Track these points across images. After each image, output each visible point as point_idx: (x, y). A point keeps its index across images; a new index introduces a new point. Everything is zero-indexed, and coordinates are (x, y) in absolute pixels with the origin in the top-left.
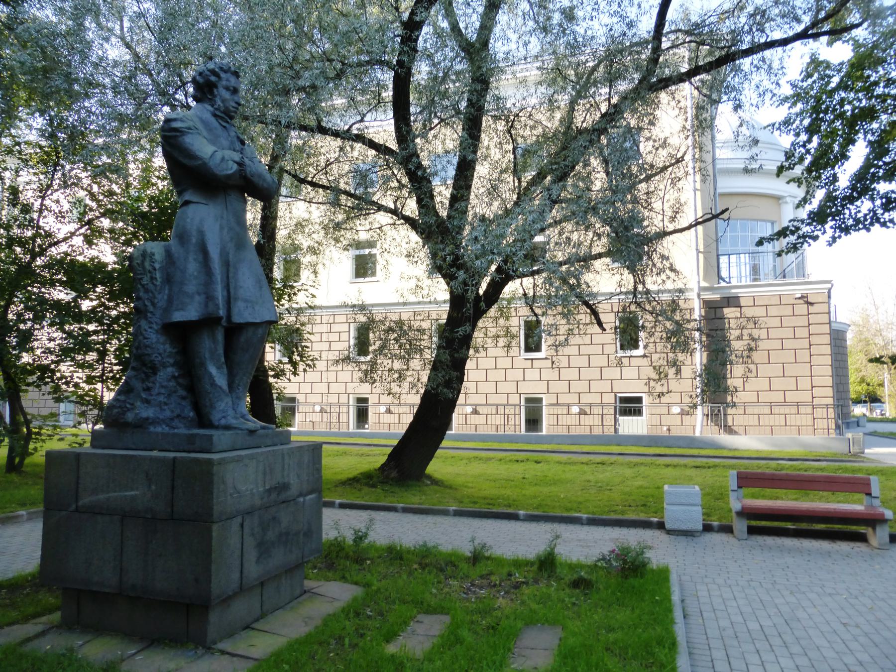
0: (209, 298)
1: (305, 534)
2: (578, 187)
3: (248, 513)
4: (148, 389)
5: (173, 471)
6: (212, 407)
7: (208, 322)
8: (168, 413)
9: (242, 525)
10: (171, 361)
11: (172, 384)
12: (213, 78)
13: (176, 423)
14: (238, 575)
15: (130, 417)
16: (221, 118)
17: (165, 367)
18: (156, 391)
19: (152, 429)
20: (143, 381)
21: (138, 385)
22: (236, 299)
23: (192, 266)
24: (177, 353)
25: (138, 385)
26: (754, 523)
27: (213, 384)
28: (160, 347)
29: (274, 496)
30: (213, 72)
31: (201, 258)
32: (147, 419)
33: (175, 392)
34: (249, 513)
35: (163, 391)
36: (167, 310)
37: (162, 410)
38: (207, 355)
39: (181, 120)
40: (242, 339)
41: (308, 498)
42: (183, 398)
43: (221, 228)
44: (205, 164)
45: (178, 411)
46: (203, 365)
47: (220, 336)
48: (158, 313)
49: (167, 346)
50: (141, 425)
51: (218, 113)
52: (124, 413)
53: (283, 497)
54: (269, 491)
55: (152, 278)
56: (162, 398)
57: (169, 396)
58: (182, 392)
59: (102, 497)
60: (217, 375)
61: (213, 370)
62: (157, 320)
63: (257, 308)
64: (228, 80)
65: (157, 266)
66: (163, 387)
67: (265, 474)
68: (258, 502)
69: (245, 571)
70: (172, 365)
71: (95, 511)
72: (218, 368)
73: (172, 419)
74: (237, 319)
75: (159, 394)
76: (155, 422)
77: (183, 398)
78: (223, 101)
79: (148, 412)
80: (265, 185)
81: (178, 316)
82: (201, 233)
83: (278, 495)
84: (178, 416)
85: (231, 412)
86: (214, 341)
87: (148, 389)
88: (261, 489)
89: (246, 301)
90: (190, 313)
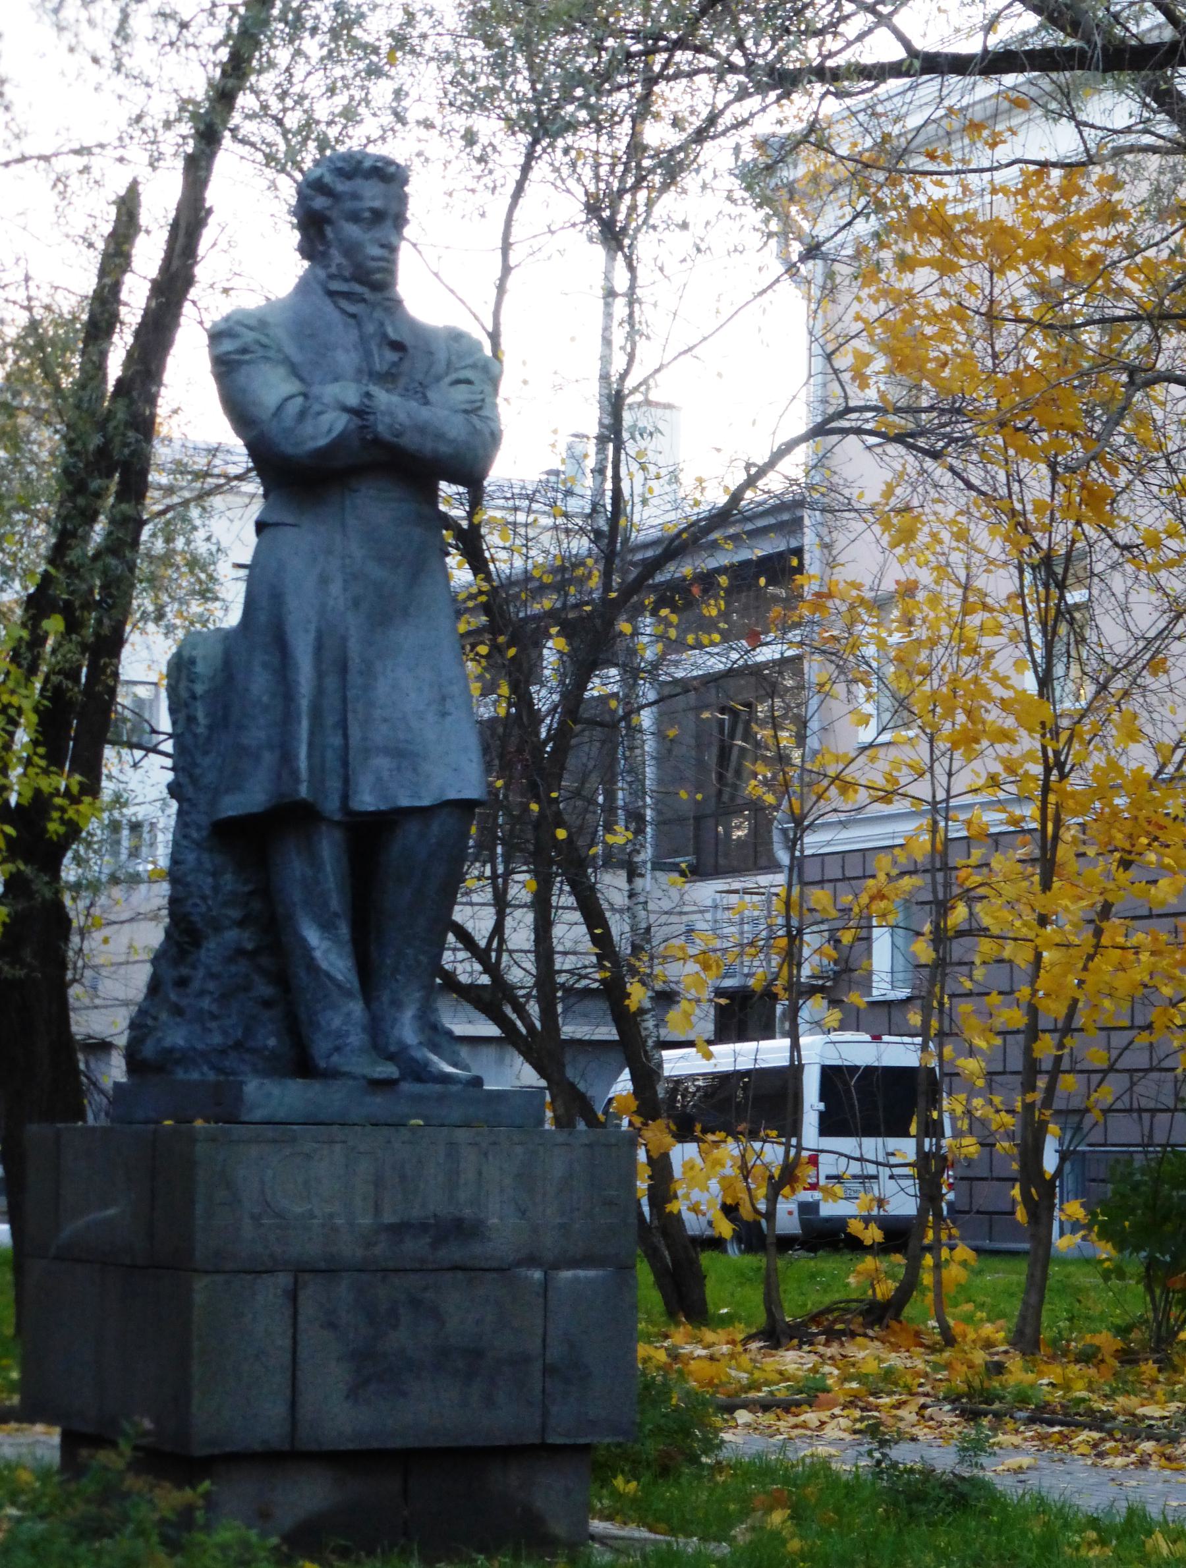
0: (287, 757)
1: (549, 1370)
8: (217, 1039)
9: (293, 1296)
10: (235, 914)
11: (242, 967)
16: (347, 295)
18: (196, 985)
19: (180, 1074)
23: (259, 683)
29: (416, 1247)
32: (171, 1050)
33: (247, 989)
34: (330, 1269)
35: (211, 986)
38: (297, 895)
41: (567, 1274)
42: (267, 1004)
47: (330, 848)
51: (335, 286)
53: (453, 1252)
54: (399, 1230)
56: (206, 1003)
58: (265, 989)
59: (80, 1223)
61: (313, 936)
64: (355, 196)
65: (199, 689)
66: (212, 976)
67: (378, 1182)
68: (350, 1249)
70: (241, 924)
73: (223, 1052)
74: (367, 800)
75: (202, 993)
77: (267, 1004)
80: (444, 449)
81: (233, 806)
83: (435, 1246)
84: (238, 1045)
86: (314, 861)
88: (366, 1221)
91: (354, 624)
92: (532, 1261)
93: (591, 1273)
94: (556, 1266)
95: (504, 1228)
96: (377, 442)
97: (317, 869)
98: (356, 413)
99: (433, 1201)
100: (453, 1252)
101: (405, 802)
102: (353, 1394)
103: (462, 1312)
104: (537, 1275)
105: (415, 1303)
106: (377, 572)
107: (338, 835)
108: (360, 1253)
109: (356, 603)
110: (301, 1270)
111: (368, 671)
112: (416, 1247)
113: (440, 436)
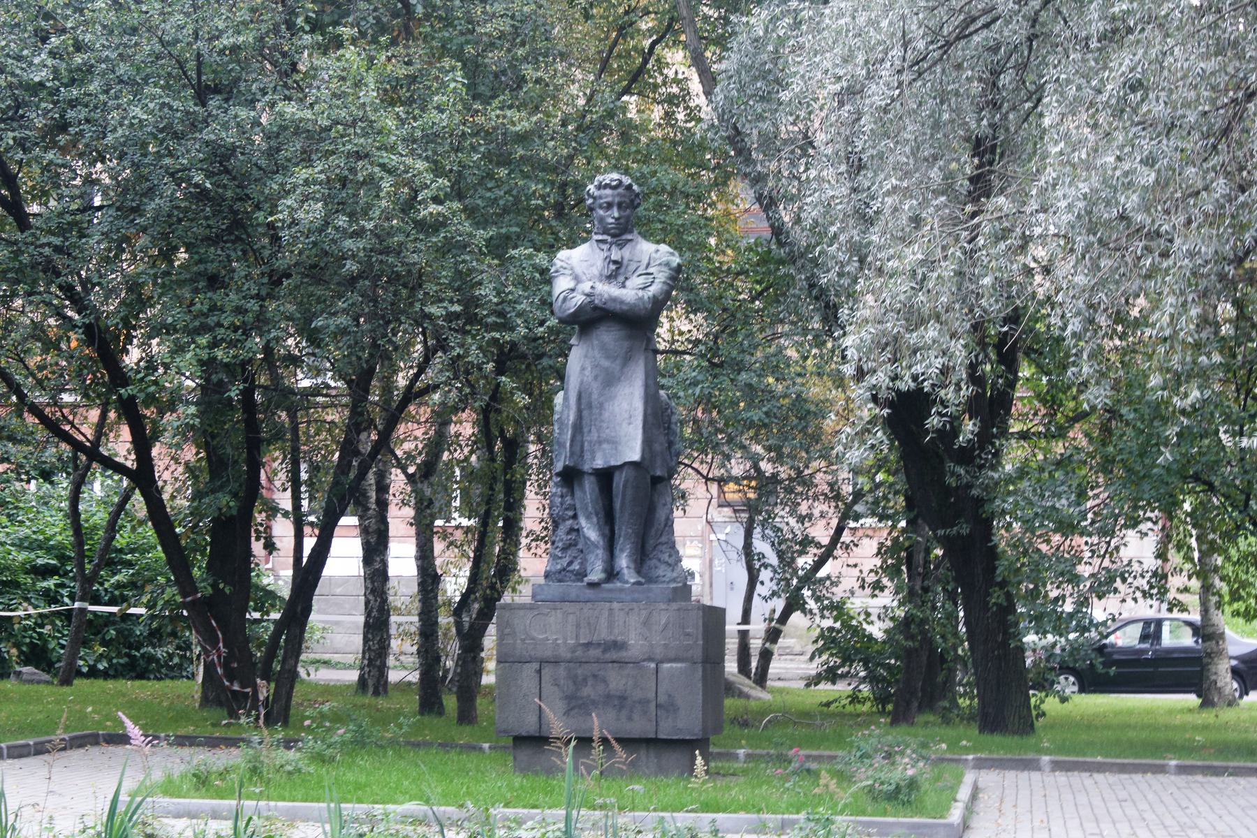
9: (539, 672)
17: (564, 520)
29: (594, 653)
53: (613, 655)
54: (588, 645)
67: (578, 626)
68: (564, 653)
72: (588, 518)
80: (625, 308)
83: (604, 652)
91: (595, 387)
92: (650, 659)
93: (679, 665)
94: (662, 662)
95: (636, 643)
96: (596, 308)
98: (588, 295)
99: (603, 634)
100: (613, 655)
101: (613, 463)
102: (567, 713)
103: (617, 681)
104: (653, 665)
105: (595, 676)
106: (606, 363)
107: (592, 478)
108: (569, 655)
109: (596, 378)
110: (543, 662)
111: (601, 406)
112: (594, 653)
113: (622, 302)
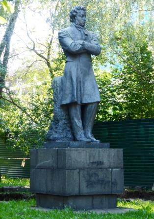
0: (73, 95)
1: (112, 183)
2: (32, 89)
3: (82, 169)
4: (56, 128)
5: (57, 153)
6: (77, 134)
7: (73, 104)
8: (62, 136)
9: (79, 172)
10: (64, 118)
11: (65, 125)
12: (74, 14)
13: (65, 139)
14: (78, 189)
15: (51, 137)
16: (78, 27)
17: (62, 120)
18: (58, 128)
19: (57, 141)
20: (55, 125)
21: (54, 127)
22: (84, 95)
23: (68, 85)
24: (66, 115)
25: (54, 127)
26: (125, 148)
27: (76, 125)
28: (61, 113)
29: (95, 166)
30: (74, 11)
31: (70, 81)
32: (55, 138)
33: (65, 129)
34: (83, 169)
35: (61, 128)
36: (61, 100)
37: (60, 135)
38: (74, 115)
39: (63, 33)
40: (88, 109)
41: (114, 169)
42: (69, 131)
43: (77, 69)
44: (69, 48)
45: (65, 135)
46: (73, 119)
47: (78, 108)
48: (59, 101)
49: (63, 113)
50: (55, 139)
51: (77, 26)
52: (50, 136)
54: (93, 163)
55: (57, 90)
56: (60, 131)
57: (63, 130)
58: (69, 129)
59: (42, 163)
60: (78, 122)
61: (76, 121)
62: (59, 104)
63: (92, 97)
64: (80, 13)
65: (58, 85)
66: (61, 127)
67: (90, 156)
69: (81, 187)
70: (65, 119)
71: (40, 168)
72: (78, 120)
73: (63, 138)
74: (84, 102)
75: (59, 129)
76: (57, 139)
77: (69, 131)
78: (79, 21)
79: (56, 136)
80: (94, 50)
81: (64, 102)
82: (70, 72)
84: (65, 137)
85: (83, 135)
86: (76, 110)
87: (56, 128)
88: (88, 162)
89: (88, 95)
90: (67, 101)
91: (81, 76)
92: (110, 168)
93: (117, 169)
94: (112, 168)
95: (106, 163)
96: (85, 49)
97: (76, 113)
98: (82, 45)
99: (97, 159)
100: (100, 166)
101: (89, 102)
102: (87, 186)
103: (101, 175)
104: (111, 169)
105: (95, 174)
106: (84, 68)
107: (80, 106)
108: (88, 167)
109: (82, 73)
110: (80, 169)
111: (84, 83)
112: (95, 166)
113: (94, 48)
